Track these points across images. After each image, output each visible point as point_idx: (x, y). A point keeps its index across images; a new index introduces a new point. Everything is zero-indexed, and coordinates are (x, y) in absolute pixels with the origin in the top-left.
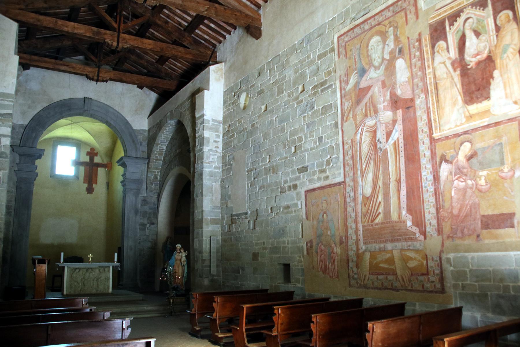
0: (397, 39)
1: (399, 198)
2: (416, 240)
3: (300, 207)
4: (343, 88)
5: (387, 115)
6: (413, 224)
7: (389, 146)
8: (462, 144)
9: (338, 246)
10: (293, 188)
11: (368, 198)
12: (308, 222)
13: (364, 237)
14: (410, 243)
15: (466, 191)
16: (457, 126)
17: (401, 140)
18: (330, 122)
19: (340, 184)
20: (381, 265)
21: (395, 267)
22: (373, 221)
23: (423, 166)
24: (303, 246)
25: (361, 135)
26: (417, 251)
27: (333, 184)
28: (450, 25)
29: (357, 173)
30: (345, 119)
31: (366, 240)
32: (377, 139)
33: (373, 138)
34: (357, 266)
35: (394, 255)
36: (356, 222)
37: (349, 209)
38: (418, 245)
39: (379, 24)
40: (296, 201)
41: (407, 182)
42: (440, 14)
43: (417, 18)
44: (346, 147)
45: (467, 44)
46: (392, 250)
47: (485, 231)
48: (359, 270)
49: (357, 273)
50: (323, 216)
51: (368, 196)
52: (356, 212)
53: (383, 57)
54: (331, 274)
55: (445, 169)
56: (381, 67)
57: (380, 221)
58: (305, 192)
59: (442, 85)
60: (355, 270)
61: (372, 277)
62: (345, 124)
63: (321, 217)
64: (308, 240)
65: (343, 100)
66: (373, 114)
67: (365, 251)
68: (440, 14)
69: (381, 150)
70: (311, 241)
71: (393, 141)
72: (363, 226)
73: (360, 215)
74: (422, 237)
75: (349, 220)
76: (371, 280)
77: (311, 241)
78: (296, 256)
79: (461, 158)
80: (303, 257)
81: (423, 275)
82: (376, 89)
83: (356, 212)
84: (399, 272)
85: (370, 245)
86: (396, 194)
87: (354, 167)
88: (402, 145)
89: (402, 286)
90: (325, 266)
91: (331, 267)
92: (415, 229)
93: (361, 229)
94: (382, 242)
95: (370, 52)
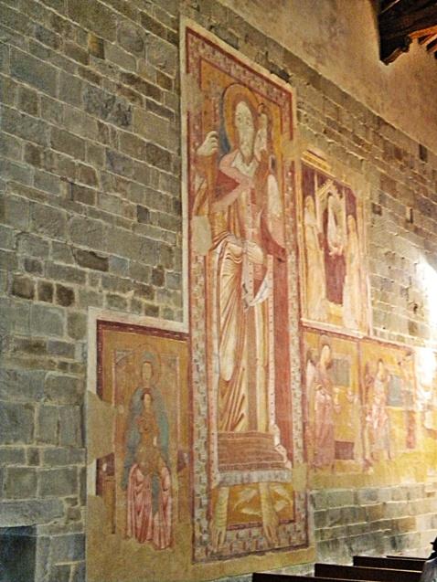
0: (270, 140)
1: (267, 397)
2: (280, 466)
3: (78, 359)
4: (192, 141)
5: (256, 251)
6: (281, 443)
7: (256, 303)
8: (323, 345)
9: (174, 474)
10: (60, 297)
11: (228, 382)
12: (101, 405)
13: (220, 456)
14: (277, 472)
15: (325, 408)
16: (319, 320)
17: (271, 305)
18: (164, 189)
19: (180, 336)
20: (244, 511)
21: (261, 513)
22: (234, 427)
23: (292, 357)
24: (84, 471)
25: (220, 259)
26: (285, 485)
27: (167, 332)
28: (319, 186)
29: (211, 330)
30: (195, 208)
31: (223, 462)
32: (242, 283)
33: (236, 277)
34: (209, 518)
35: (261, 492)
36: (207, 423)
37: (197, 396)
38: (286, 476)
39: (250, 89)
40: (66, 339)
41: (276, 374)
42: (310, 160)
43: (291, 138)
44: (193, 266)
45: (329, 224)
46: (258, 483)
47: (337, 460)
48: (211, 523)
49: (208, 532)
50: (143, 398)
51: (228, 379)
52: (208, 405)
53: (253, 153)
54: (157, 541)
55: (310, 369)
56: (251, 164)
57: (244, 431)
58: (99, 322)
59: (310, 254)
60: (204, 523)
61: (230, 534)
62: (195, 218)
63: (137, 399)
64: (101, 455)
65: (193, 167)
66: (238, 235)
67: (221, 484)
68: (310, 160)
69: (247, 305)
70: (110, 458)
71: (261, 301)
72: (219, 436)
73: (214, 411)
74: (289, 465)
75: (198, 420)
76: (229, 541)
77: (110, 458)
78: (62, 498)
79: (322, 363)
80: (84, 502)
81: (291, 521)
82: (243, 194)
83: (208, 405)
84: (265, 521)
85: (228, 473)
86: (263, 389)
87: (207, 313)
88: (271, 312)
89: (269, 545)
90: (145, 522)
91: (157, 523)
92: (282, 451)
93: (214, 438)
94: (242, 470)
95: (237, 123)
